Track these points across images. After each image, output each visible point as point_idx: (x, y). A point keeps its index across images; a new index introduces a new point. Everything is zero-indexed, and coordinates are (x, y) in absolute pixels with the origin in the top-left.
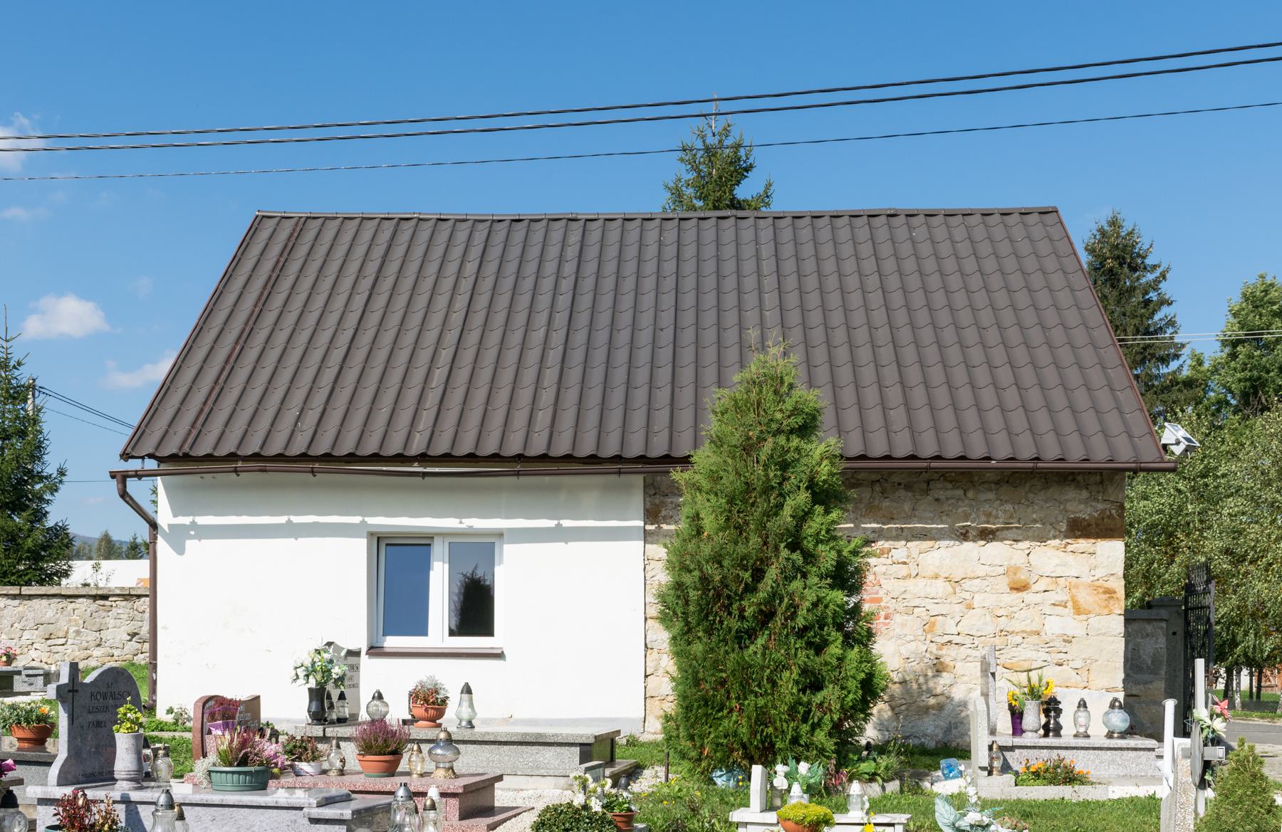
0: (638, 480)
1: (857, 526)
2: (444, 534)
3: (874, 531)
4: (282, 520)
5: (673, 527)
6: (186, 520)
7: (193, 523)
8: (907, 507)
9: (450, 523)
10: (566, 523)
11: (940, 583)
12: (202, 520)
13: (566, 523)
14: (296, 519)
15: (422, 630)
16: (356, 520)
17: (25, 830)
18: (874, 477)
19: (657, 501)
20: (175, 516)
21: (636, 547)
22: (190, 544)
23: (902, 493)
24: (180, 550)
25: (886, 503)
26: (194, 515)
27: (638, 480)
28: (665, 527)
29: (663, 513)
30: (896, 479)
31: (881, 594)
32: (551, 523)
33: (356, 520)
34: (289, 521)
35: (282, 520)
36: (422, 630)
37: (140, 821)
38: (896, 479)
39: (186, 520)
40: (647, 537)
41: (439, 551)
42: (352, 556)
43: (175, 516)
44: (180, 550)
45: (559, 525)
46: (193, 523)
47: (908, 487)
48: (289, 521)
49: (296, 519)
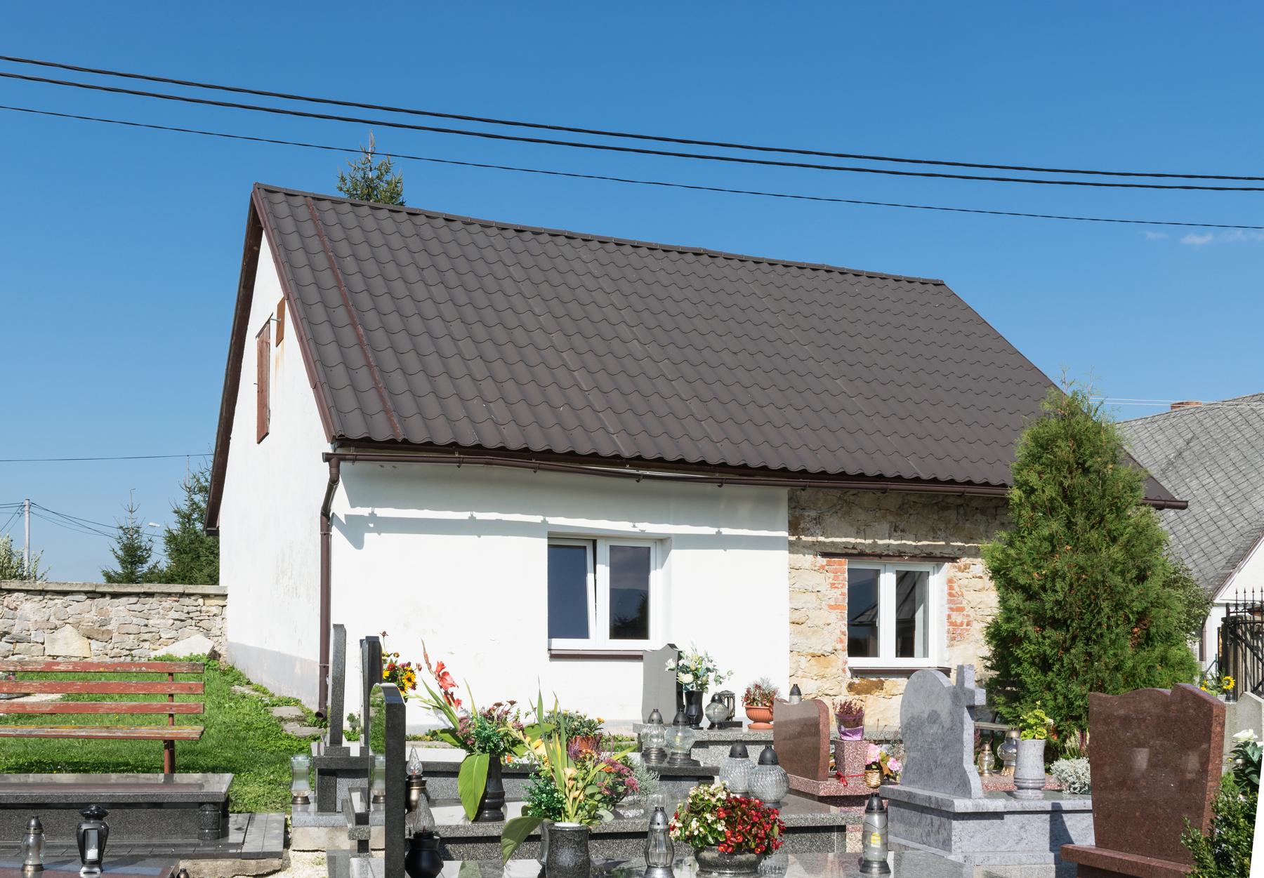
0: (783, 493)
1: (947, 544)
2: (608, 536)
3: (960, 548)
4: (465, 515)
5: (810, 539)
6: (364, 511)
7: (372, 514)
8: (982, 529)
9: (624, 526)
10: (726, 531)
11: (808, 596)
12: (382, 512)
13: (726, 531)
14: (480, 516)
15: (583, 633)
16: (538, 519)
17: (324, 870)
18: (959, 501)
19: (797, 514)
20: (353, 506)
21: (782, 557)
22: (369, 537)
23: (979, 516)
24: (358, 543)
25: (968, 525)
26: (373, 506)
27: (783, 493)
28: (804, 538)
29: (802, 525)
30: (975, 504)
31: (964, 604)
32: (711, 531)
33: (538, 519)
34: (472, 517)
35: (465, 515)
36: (583, 633)
37: (1066, 831)
38: (975, 504)
39: (364, 511)
40: (793, 547)
41: (603, 551)
42: (533, 557)
43: (353, 506)
44: (358, 543)
45: (719, 533)
46: (372, 514)
47: (983, 512)
48: (472, 517)
49: (480, 516)
